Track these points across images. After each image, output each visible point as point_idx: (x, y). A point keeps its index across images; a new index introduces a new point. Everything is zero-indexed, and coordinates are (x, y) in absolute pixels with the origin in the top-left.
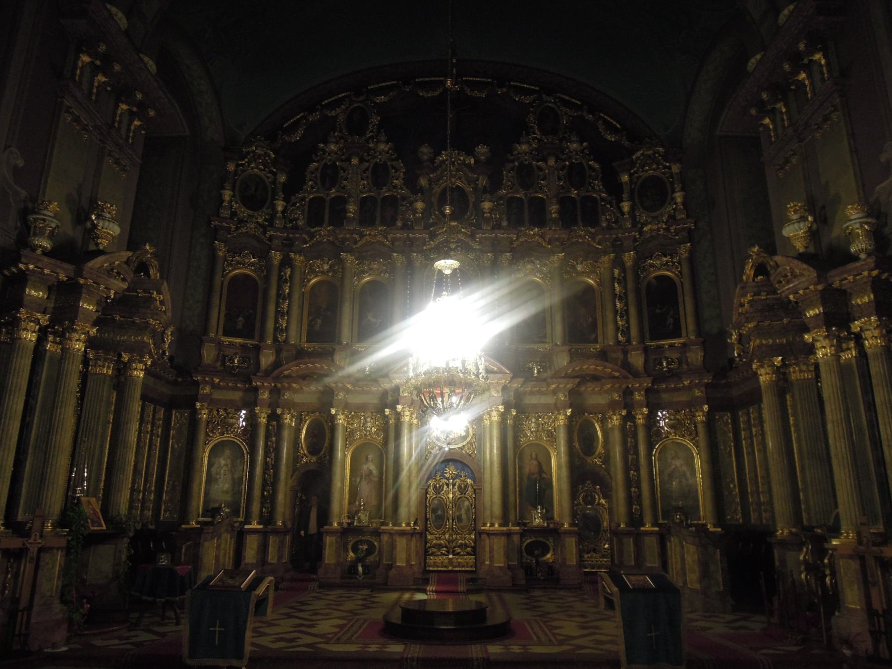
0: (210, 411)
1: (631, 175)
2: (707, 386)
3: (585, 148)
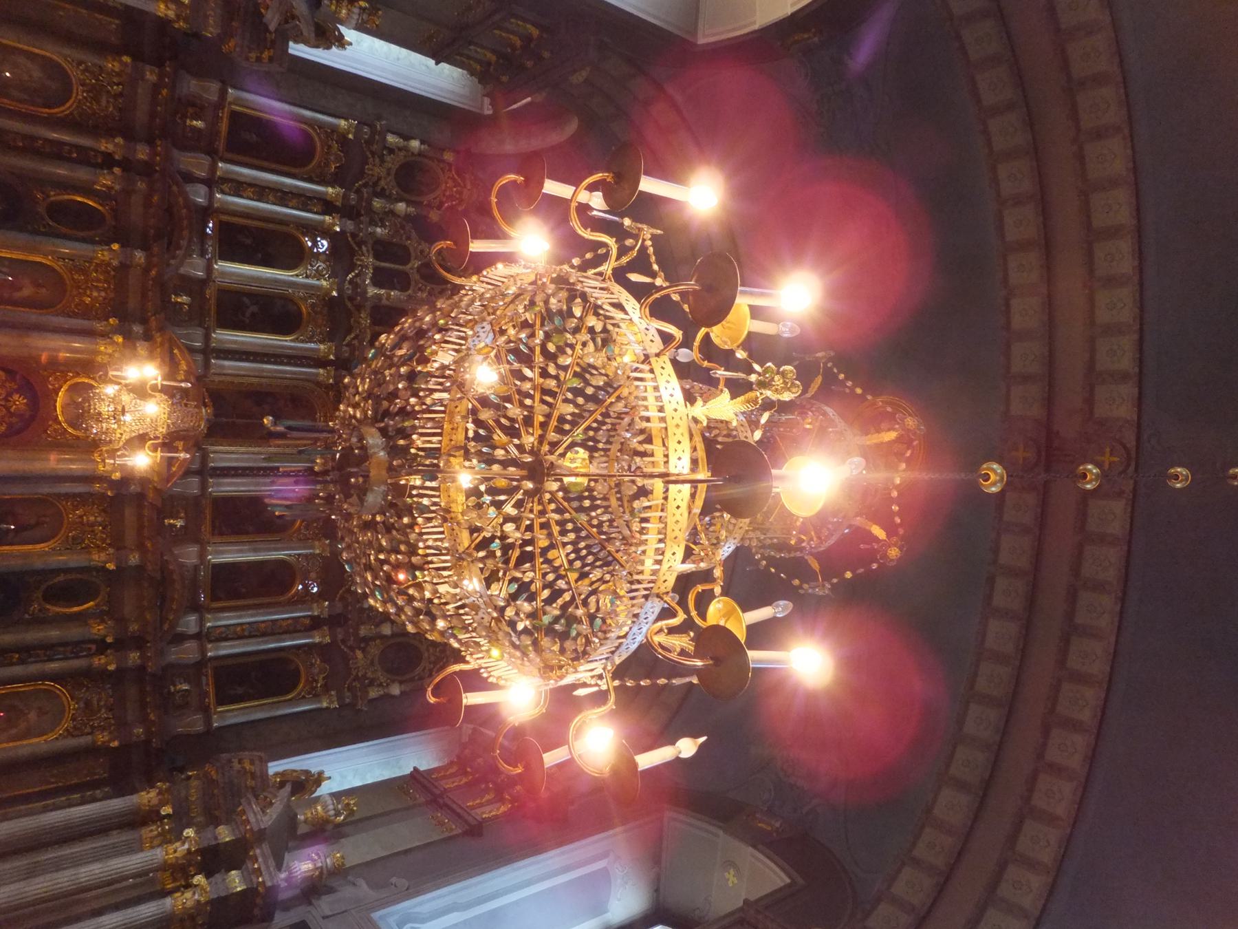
0: (118, 74)
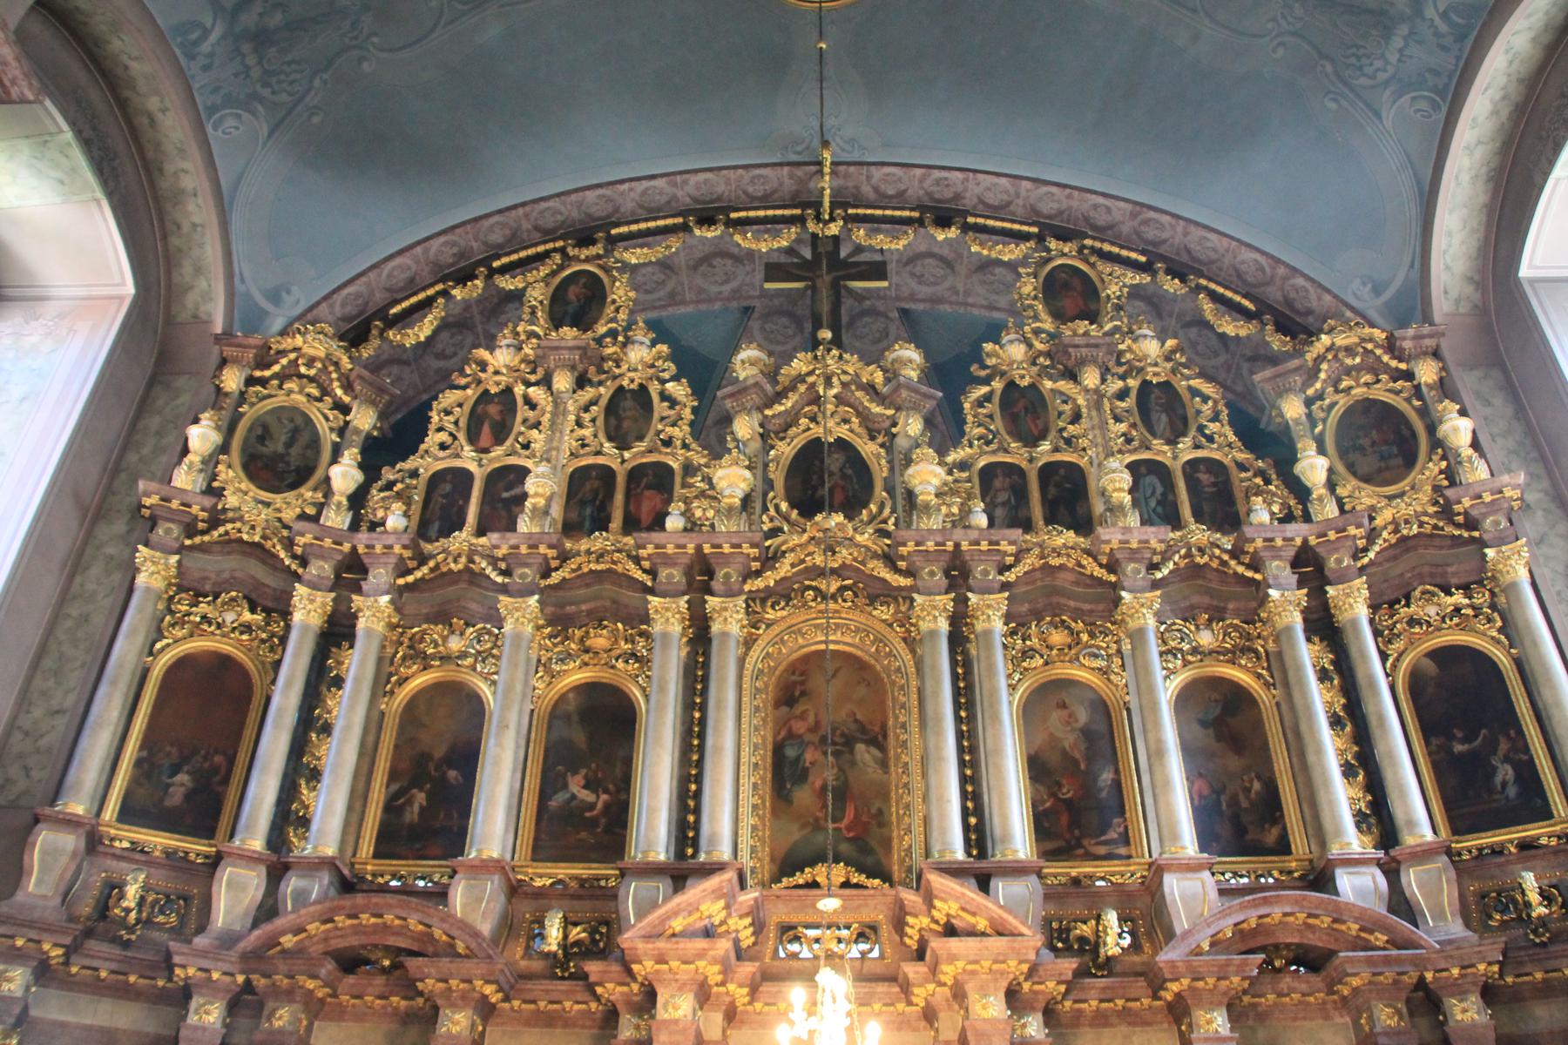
1: (1309, 403)
3: (1173, 352)
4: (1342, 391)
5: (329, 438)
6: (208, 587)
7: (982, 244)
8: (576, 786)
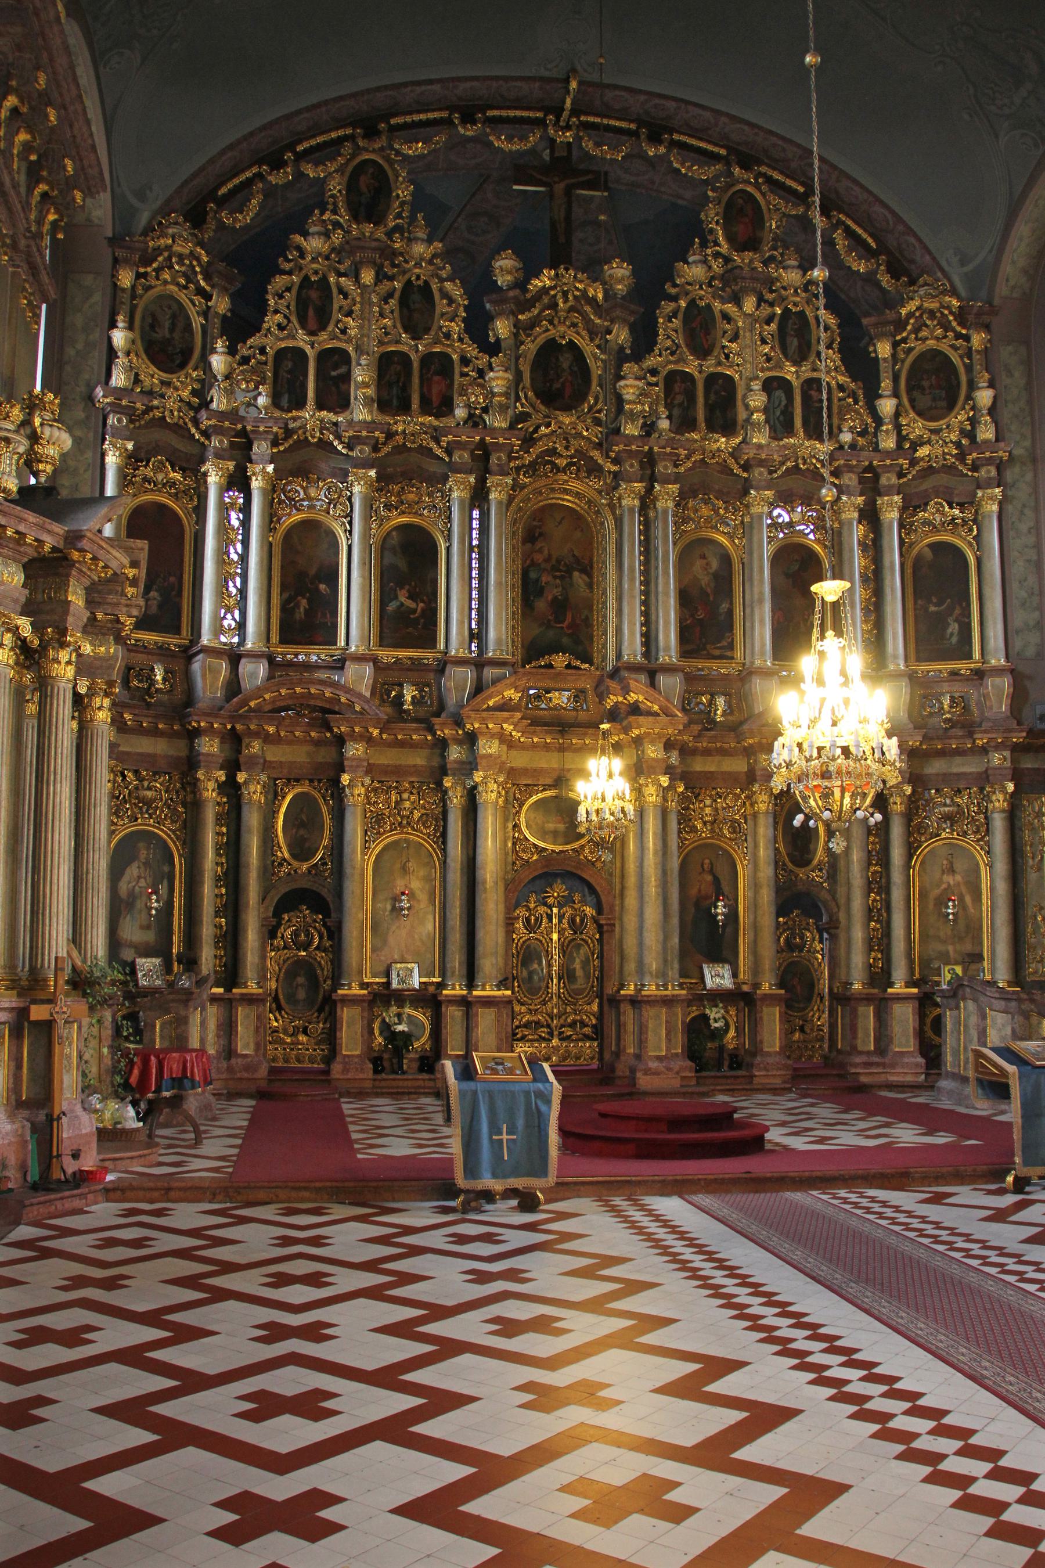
1: (895, 345)
2: (1015, 749)
4: (920, 339)
5: (197, 321)
6: (143, 455)
7: (683, 165)
8: (403, 597)
